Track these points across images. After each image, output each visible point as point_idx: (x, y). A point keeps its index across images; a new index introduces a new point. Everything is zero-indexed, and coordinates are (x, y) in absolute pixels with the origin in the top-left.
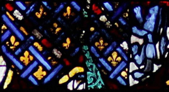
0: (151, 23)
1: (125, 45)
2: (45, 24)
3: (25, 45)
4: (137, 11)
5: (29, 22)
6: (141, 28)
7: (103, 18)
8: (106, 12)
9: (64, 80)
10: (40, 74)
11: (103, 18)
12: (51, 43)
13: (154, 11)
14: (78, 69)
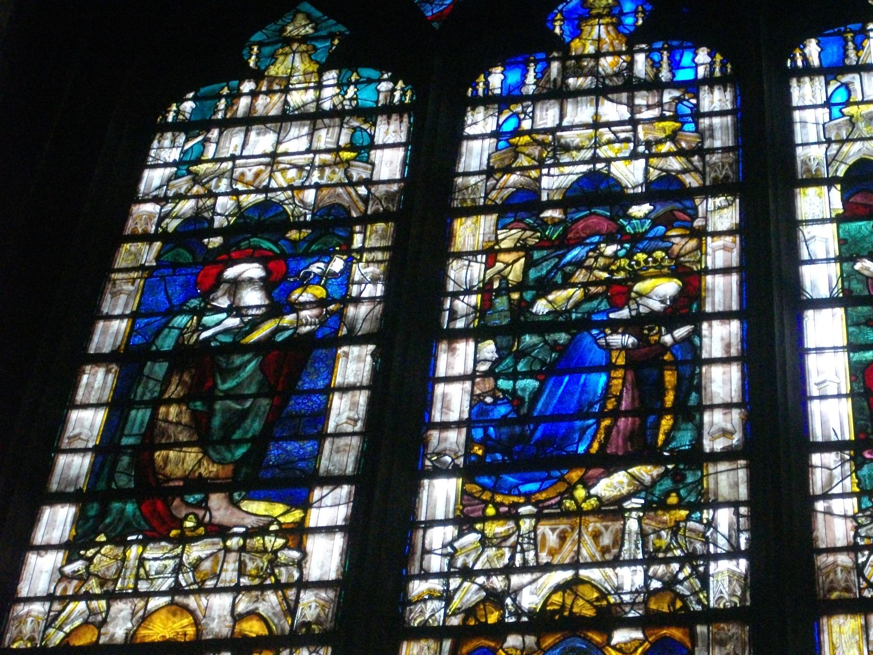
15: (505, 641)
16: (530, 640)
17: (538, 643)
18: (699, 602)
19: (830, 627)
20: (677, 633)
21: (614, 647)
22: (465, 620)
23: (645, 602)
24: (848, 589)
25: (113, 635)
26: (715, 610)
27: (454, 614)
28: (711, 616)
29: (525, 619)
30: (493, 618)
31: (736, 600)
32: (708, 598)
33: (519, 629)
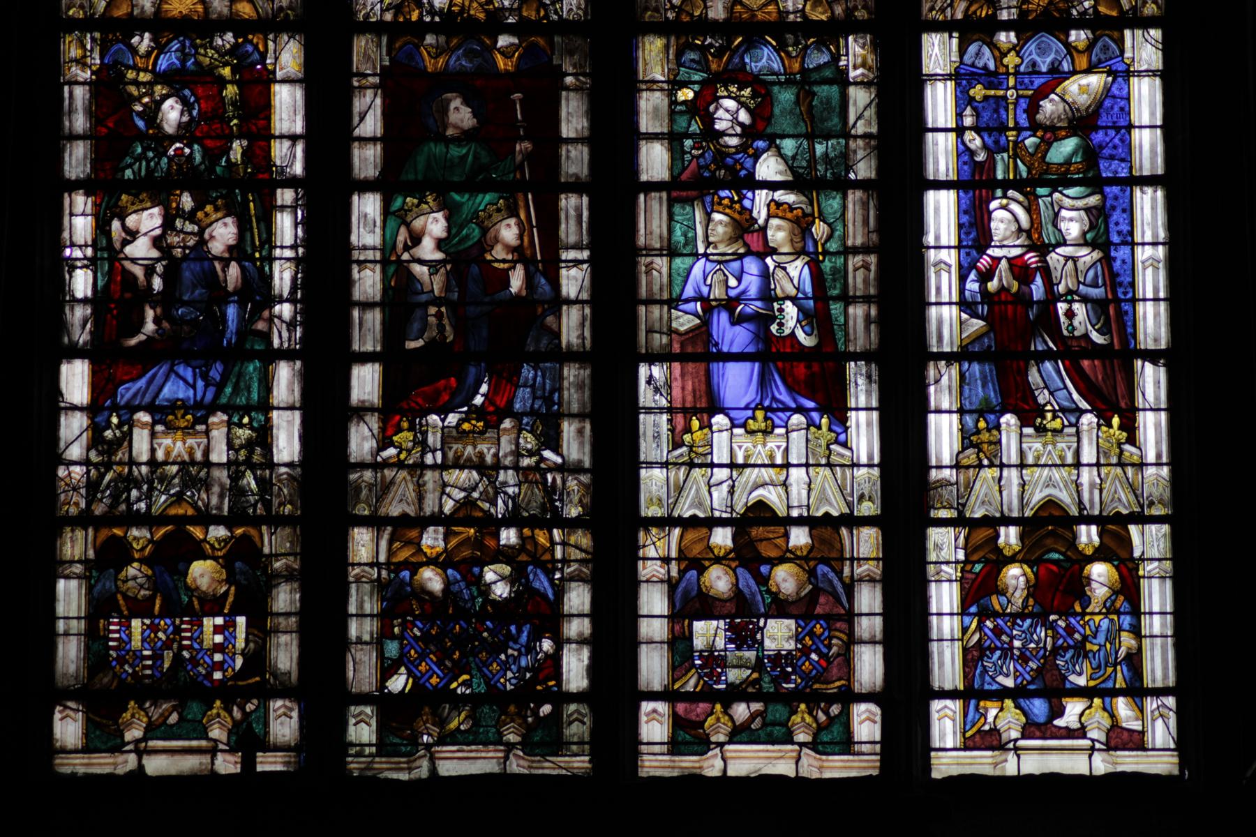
0: (524, 638)
1: (503, 657)
2: (438, 640)
3: (422, 657)
4: (513, 628)
5: (426, 638)
6: (516, 642)
7: (485, 634)
8: (487, 630)
9: (454, 685)
10: (434, 680)
11: (485, 634)
12: (443, 655)
13: (526, 630)
14: (465, 677)
15: (424, 39)
16: (442, 39)
17: (447, 43)
18: (556, 12)
19: (644, 44)
20: (541, 41)
21: (498, 50)
22: (395, 16)
23: (520, 9)
24: (657, 10)
25: (143, 7)
26: (567, 20)
27: (388, 9)
28: (565, 26)
29: (437, 19)
30: (415, 16)
31: (580, 12)
32: (561, 8)
33: (432, 28)
